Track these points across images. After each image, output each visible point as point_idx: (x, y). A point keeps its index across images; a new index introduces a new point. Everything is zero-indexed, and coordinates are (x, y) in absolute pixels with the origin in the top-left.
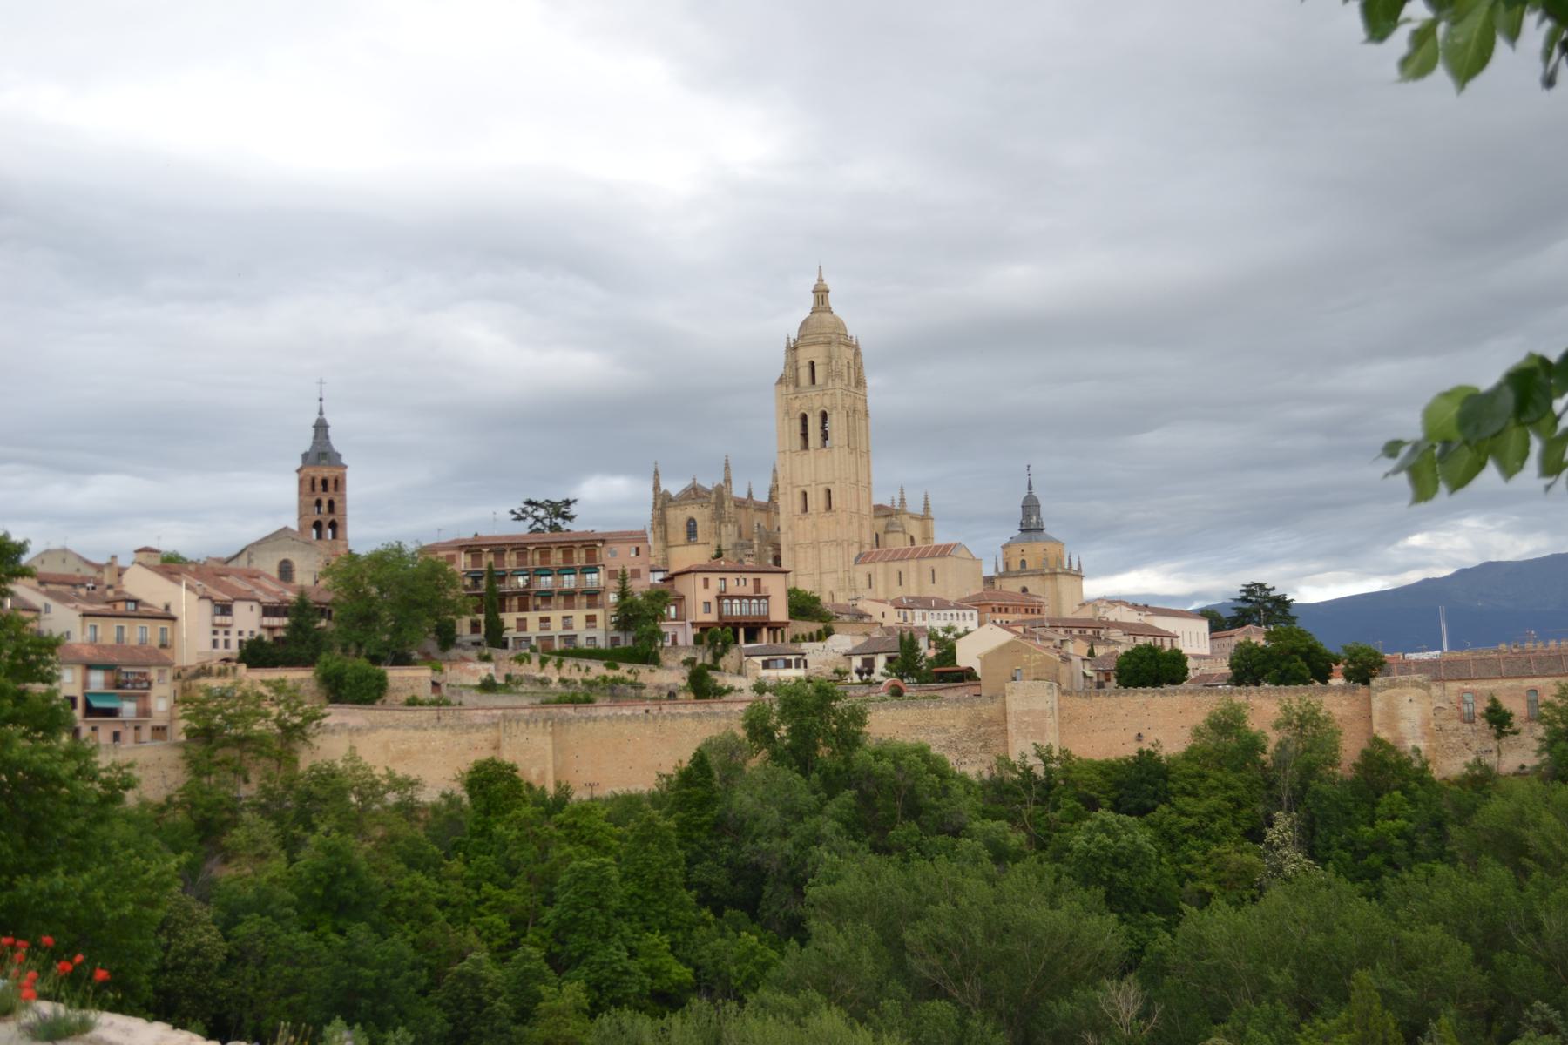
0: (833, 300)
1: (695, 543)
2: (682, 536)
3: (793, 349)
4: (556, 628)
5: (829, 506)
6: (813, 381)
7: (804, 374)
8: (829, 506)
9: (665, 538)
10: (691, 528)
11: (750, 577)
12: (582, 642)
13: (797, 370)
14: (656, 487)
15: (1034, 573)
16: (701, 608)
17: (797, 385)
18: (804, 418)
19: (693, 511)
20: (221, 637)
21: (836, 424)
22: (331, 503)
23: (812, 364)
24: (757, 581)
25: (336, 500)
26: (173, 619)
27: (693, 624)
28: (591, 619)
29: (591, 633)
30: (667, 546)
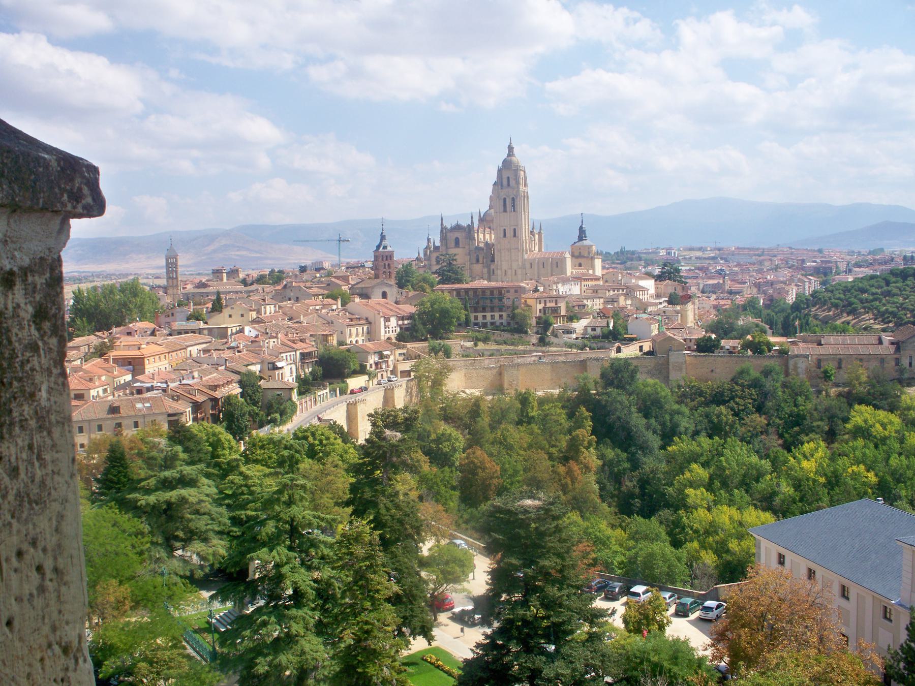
0: (515, 151)
1: (458, 247)
2: (453, 244)
3: (500, 171)
4: (489, 319)
5: (515, 236)
6: (509, 185)
7: (505, 182)
8: (515, 236)
9: (446, 245)
10: (457, 242)
11: (554, 299)
12: (498, 324)
13: (502, 179)
14: (442, 224)
15: (584, 257)
16: (538, 311)
17: (502, 185)
18: (505, 200)
19: (458, 234)
20: (387, 329)
21: (517, 202)
22: (389, 264)
23: (508, 178)
24: (556, 301)
25: (391, 263)
26: (370, 323)
27: (536, 317)
28: (501, 316)
29: (501, 321)
30: (447, 248)
